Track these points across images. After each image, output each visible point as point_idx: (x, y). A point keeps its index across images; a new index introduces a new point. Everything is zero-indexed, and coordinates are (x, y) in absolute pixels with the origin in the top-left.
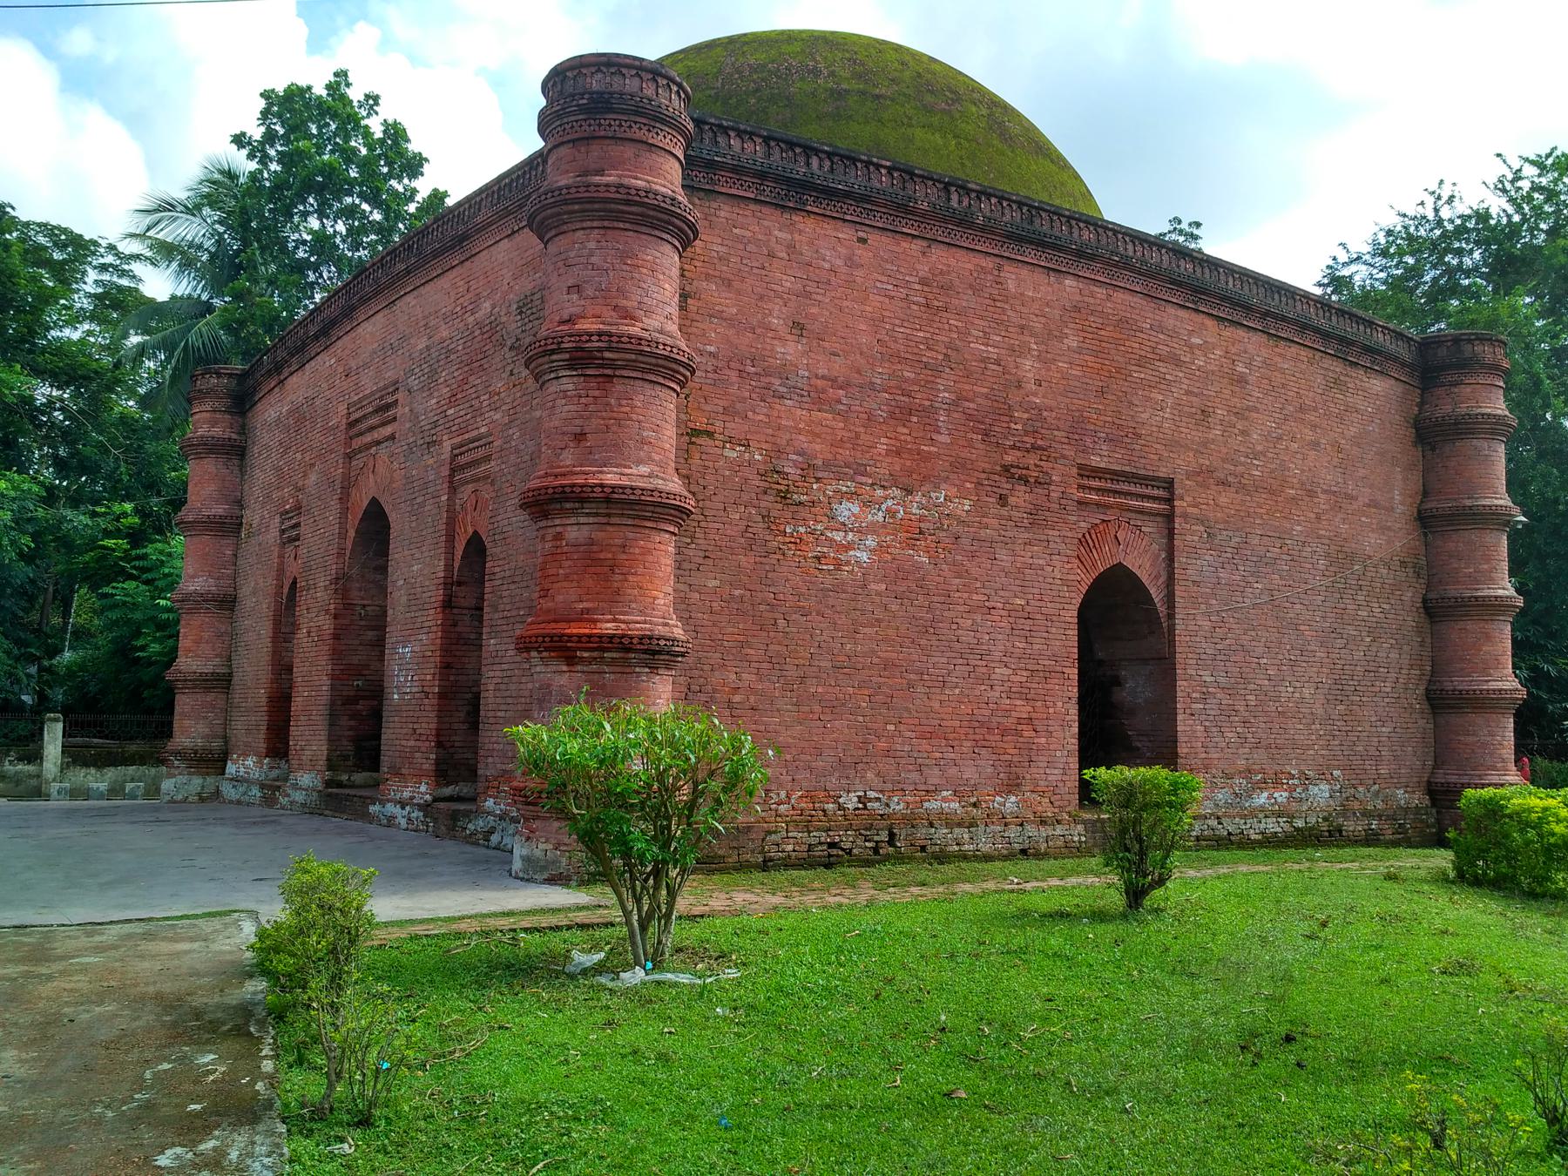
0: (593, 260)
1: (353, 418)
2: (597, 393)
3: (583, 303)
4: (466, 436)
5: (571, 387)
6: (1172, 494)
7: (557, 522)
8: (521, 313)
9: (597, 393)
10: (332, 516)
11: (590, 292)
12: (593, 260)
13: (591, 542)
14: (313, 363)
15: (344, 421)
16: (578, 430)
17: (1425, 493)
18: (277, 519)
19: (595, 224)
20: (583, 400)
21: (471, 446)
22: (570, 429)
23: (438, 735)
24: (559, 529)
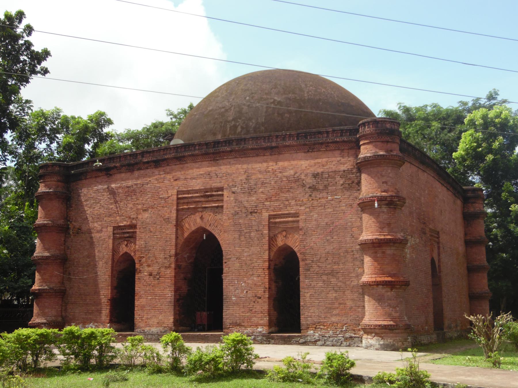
0: (390, 175)
1: (180, 196)
2: (393, 213)
3: (388, 187)
4: (280, 213)
5: (385, 210)
6: (439, 236)
7: (384, 248)
8: (315, 177)
9: (393, 213)
10: (170, 231)
11: (389, 184)
12: (390, 175)
13: (394, 254)
14: (142, 172)
15: (175, 197)
16: (388, 223)
17: (466, 234)
18: (110, 229)
19: (391, 165)
20: (389, 214)
21: (282, 216)
22: (386, 222)
23: (268, 311)
24: (383, 250)
